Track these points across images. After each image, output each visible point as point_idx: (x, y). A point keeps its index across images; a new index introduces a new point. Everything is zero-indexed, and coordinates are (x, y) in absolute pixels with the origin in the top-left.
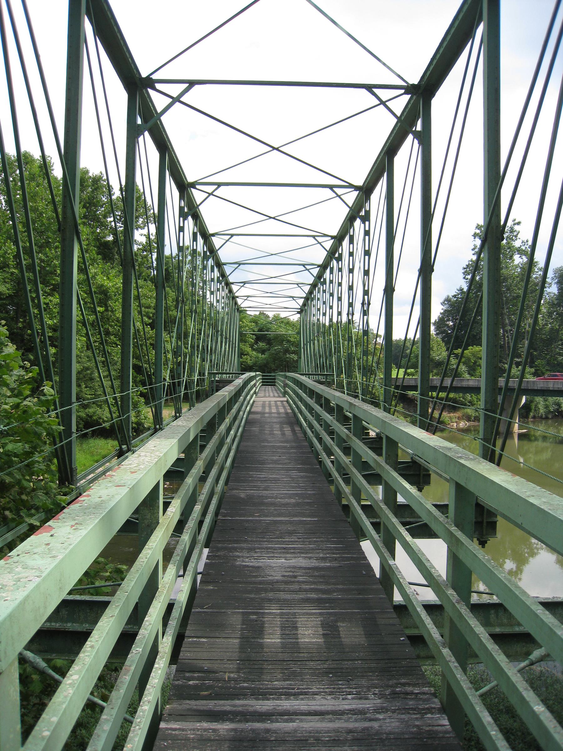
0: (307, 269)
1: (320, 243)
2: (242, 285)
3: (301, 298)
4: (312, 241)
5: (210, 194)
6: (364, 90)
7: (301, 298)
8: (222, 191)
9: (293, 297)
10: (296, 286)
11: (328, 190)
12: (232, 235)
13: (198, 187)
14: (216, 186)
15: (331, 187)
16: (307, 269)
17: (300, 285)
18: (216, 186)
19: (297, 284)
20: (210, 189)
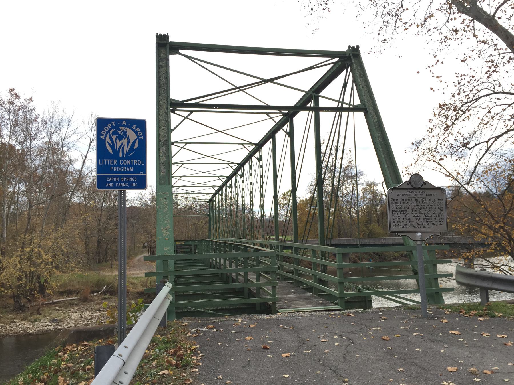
0: (220, 179)
1: (231, 167)
2: (178, 187)
3: (212, 194)
4: (227, 166)
5: (182, 148)
6: (265, 115)
7: (212, 194)
8: (188, 146)
9: (206, 193)
10: (211, 187)
11: (241, 145)
12: (183, 164)
13: (174, 144)
14: (185, 144)
15: (243, 144)
16: (220, 179)
17: (213, 187)
18: (185, 144)
19: (212, 186)
20: (182, 145)
